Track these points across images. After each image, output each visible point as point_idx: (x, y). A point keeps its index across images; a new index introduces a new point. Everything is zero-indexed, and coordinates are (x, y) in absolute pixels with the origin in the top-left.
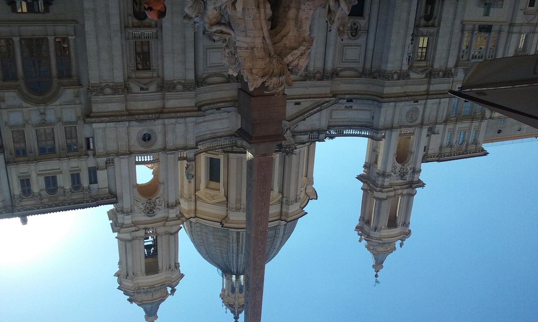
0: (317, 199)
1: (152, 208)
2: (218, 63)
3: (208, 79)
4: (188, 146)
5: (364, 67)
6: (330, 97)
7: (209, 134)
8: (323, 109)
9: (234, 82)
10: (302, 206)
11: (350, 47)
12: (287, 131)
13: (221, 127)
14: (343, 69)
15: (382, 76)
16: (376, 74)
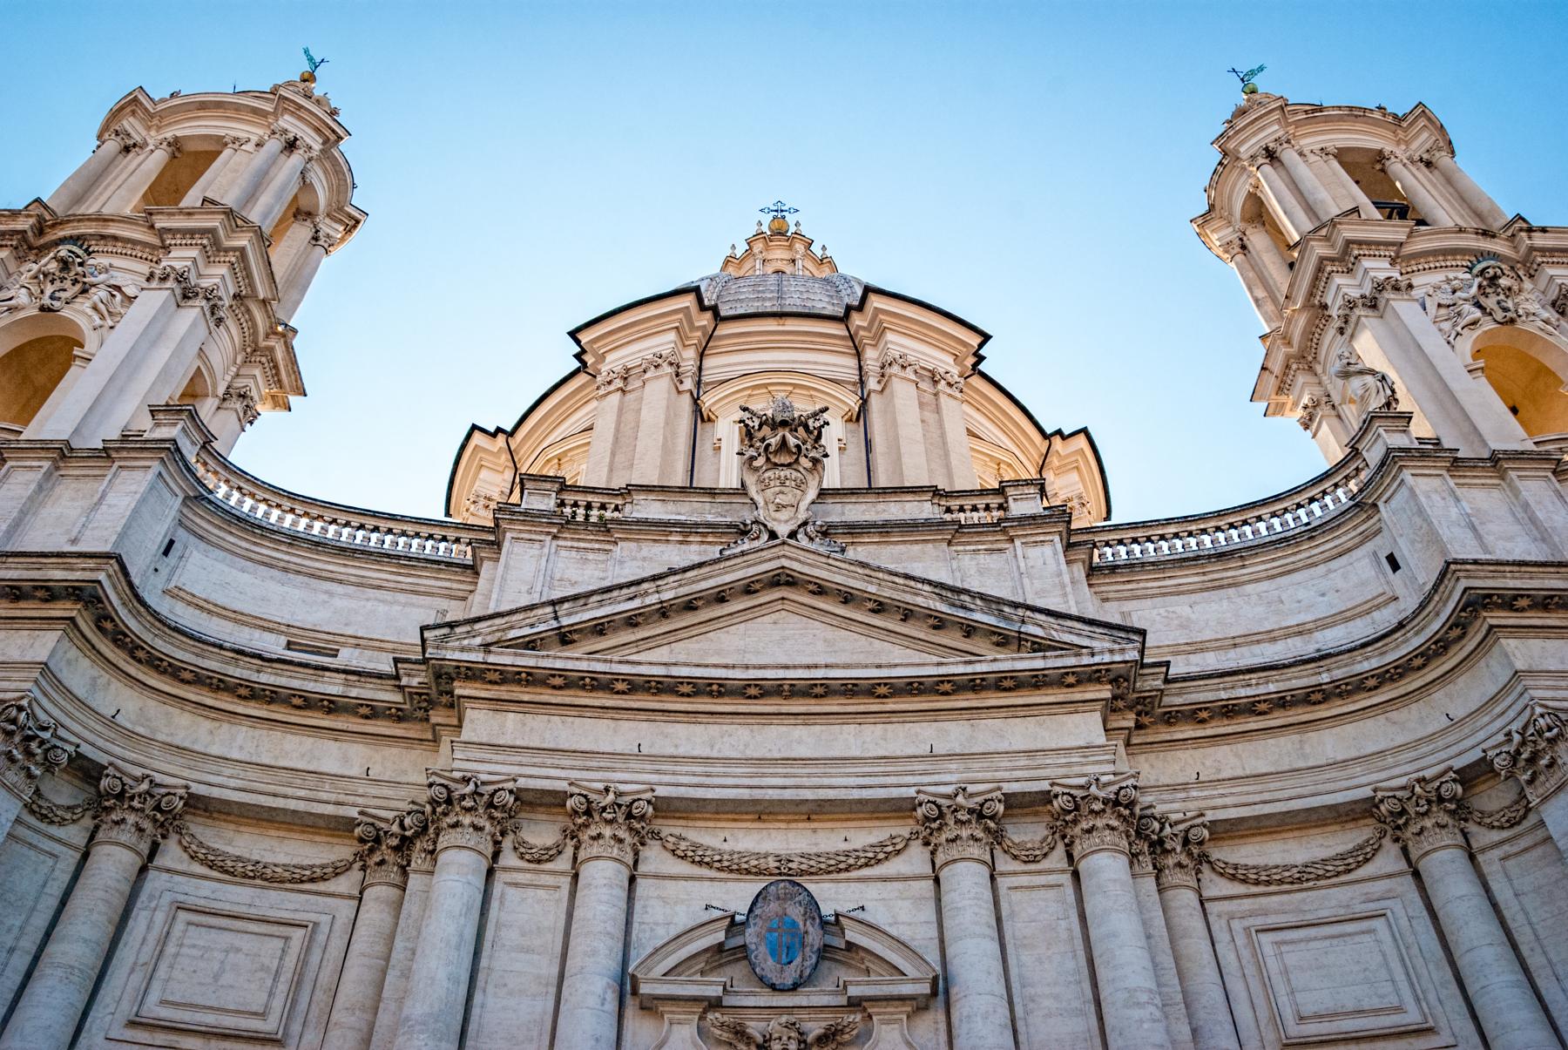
0: (474, 427)
1: (1488, 290)
2: (1309, 940)
3: (1350, 846)
4: (1444, 472)
5: (143, 870)
6: (472, 673)
7: (1250, 582)
8: (543, 604)
9: (1177, 823)
10: (582, 379)
11: (229, 1022)
12: (793, 535)
13: (1184, 610)
14: (312, 880)
15: (34, 745)
16: (62, 792)
